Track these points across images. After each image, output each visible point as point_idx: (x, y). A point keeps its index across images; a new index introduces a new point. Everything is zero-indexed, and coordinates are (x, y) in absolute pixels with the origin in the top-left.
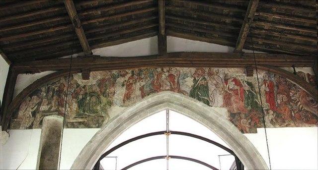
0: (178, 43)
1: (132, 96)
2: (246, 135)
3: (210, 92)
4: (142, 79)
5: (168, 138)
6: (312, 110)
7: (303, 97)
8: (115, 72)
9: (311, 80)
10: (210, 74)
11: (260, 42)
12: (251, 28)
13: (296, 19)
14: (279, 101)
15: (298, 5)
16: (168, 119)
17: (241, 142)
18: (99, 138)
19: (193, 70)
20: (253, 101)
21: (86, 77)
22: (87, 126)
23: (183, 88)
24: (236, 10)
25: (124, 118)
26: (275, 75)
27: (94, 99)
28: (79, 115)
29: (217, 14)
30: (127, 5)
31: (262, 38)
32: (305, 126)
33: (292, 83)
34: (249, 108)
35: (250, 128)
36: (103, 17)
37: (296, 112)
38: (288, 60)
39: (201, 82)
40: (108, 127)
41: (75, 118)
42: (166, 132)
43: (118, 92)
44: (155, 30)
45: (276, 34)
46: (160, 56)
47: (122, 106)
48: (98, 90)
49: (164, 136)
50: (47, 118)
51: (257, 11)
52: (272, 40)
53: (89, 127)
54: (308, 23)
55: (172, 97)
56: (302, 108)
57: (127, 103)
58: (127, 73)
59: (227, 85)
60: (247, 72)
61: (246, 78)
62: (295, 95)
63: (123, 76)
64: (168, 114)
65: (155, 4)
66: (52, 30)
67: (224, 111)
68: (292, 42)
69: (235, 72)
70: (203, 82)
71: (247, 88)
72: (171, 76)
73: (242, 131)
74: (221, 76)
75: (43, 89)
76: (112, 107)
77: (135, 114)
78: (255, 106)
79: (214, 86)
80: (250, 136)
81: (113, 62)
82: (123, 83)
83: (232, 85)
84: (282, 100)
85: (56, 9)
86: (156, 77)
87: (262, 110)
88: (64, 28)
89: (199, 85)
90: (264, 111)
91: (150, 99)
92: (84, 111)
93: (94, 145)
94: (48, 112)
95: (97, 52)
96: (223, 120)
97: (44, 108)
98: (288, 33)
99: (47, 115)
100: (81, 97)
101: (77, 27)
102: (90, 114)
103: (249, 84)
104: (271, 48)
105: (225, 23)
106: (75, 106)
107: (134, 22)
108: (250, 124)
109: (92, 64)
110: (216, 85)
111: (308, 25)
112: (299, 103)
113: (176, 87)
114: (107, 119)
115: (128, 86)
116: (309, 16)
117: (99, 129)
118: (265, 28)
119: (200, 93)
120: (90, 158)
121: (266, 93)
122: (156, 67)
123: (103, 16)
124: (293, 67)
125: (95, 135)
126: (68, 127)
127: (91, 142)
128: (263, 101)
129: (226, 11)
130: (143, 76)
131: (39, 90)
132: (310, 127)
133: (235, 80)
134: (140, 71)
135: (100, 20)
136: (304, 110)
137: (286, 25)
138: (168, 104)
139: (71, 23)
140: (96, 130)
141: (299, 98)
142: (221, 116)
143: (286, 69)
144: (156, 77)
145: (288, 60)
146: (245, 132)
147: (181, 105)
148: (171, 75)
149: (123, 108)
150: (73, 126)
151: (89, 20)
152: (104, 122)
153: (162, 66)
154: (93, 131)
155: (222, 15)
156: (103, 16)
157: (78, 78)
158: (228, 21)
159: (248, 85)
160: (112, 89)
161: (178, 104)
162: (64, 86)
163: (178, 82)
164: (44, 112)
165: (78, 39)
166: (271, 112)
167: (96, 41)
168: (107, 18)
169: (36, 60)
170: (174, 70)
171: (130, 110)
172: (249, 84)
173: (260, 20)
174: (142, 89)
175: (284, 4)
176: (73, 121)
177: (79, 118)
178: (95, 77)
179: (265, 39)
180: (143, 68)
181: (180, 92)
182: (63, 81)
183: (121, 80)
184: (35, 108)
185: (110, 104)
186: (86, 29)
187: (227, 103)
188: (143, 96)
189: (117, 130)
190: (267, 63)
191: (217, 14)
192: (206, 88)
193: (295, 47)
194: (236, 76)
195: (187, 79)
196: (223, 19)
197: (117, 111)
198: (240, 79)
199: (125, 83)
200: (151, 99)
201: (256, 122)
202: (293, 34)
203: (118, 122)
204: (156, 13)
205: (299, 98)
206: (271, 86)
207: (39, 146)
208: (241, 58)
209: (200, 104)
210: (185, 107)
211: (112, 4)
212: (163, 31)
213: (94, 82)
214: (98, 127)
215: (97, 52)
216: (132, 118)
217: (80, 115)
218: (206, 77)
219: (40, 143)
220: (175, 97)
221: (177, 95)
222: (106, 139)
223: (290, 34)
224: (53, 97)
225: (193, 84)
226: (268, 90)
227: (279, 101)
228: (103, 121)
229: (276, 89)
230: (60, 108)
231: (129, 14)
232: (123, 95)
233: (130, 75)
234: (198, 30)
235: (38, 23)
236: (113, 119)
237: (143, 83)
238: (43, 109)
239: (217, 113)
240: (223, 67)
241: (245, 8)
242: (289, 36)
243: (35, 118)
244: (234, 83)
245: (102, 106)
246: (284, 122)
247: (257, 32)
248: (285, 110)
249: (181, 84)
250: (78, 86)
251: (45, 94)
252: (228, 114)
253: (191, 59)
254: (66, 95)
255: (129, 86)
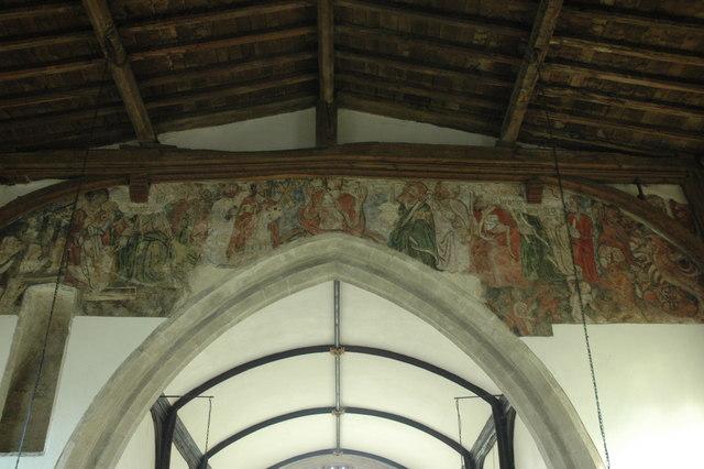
0: (363, 125)
1: (249, 243)
2: (525, 339)
3: (439, 239)
4: (275, 203)
5: (338, 364)
6: (684, 282)
7: (661, 253)
8: (210, 186)
9: (680, 215)
10: (440, 196)
11: (558, 125)
12: (541, 84)
13: (650, 56)
14: (604, 262)
15: (657, 15)
16: (337, 313)
17: (513, 356)
18: (163, 341)
19: (398, 185)
20: (541, 259)
21: (139, 195)
22: (134, 310)
23: (374, 227)
24: (508, 32)
25: (226, 296)
26: (593, 202)
27: (155, 248)
28: (116, 285)
29: (458, 45)
30: (240, 13)
31: (563, 111)
32: (668, 321)
33: (633, 222)
34: (534, 276)
35: (536, 324)
36: (184, 43)
37: (645, 287)
38: (625, 167)
39: (417, 213)
40: (184, 320)
41: (107, 290)
42: (333, 346)
43: (215, 234)
44: (309, 93)
45: (598, 99)
46: (320, 149)
47: (224, 266)
48: (168, 226)
49: (327, 357)
50: (35, 290)
51: (558, 33)
52: (587, 116)
53: (140, 314)
54: (678, 64)
55: (347, 248)
56: (659, 278)
57: (235, 258)
58: (239, 189)
59: (479, 221)
60: (528, 193)
61: (525, 207)
62: (643, 249)
63: (231, 195)
64: (337, 298)
65: (310, 18)
66: (53, 70)
67: (473, 283)
68: (635, 120)
69: (500, 193)
70: (424, 215)
71: (527, 229)
72: (346, 199)
73: (517, 332)
74: (466, 202)
75: (33, 221)
76: (199, 268)
77: (256, 287)
78: (548, 271)
79: (449, 225)
80: (534, 344)
81: (206, 162)
82: (229, 211)
83: (491, 222)
84: (612, 258)
85: (61, 10)
86: (308, 200)
87: (565, 282)
88: (83, 66)
89: (413, 220)
90: (570, 284)
91: (292, 252)
92: (130, 276)
93: (150, 358)
94: (39, 277)
95: (171, 138)
96: (470, 304)
97: (29, 265)
98: (627, 97)
99: (37, 283)
100: (123, 242)
101: (115, 62)
102: (142, 281)
103: (533, 221)
104: (584, 138)
105: (476, 71)
106: (107, 263)
107: (258, 65)
108: (535, 314)
109: (158, 163)
110: (453, 222)
111: (676, 72)
112: (653, 267)
113: (356, 224)
114: (186, 295)
115: (242, 218)
116: (683, 46)
117: (164, 319)
118: (572, 84)
119: (413, 238)
120: (137, 391)
121: (572, 242)
122: (310, 177)
123: (183, 39)
124: (637, 182)
125: (153, 336)
126: (85, 312)
127: (141, 349)
128: (563, 260)
129: (480, 34)
130: (277, 197)
131: (22, 223)
132: (680, 323)
133: (499, 211)
134: (273, 184)
135: (174, 51)
136: (665, 282)
137: (625, 72)
138: (337, 266)
139: (100, 56)
140: (153, 323)
141: (651, 255)
142: (464, 293)
143: (620, 187)
144: (308, 200)
145: (625, 167)
146: (522, 332)
147: (368, 268)
148: (346, 195)
149: (224, 271)
150: (99, 309)
151: (148, 49)
152: (178, 304)
153: (325, 173)
154: (149, 324)
155: (470, 47)
156: (183, 39)
157: (120, 198)
158: (484, 63)
159: (530, 223)
160: (202, 226)
161: (361, 266)
162: (86, 216)
163: (362, 212)
164: (30, 274)
165: (121, 103)
166: (586, 287)
167: (165, 117)
168: (192, 48)
169: (18, 150)
170: (353, 185)
171: (241, 276)
172: (533, 221)
173: (560, 61)
174: (273, 227)
175: (625, 12)
176: (102, 298)
177: (117, 291)
178: (163, 195)
179: (571, 113)
180: (278, 178)
181: (366, 234)
182: (82, 203)
183: (224, 205)
184: (8, 265)
185: (195, 259)
186: (140, 75)
187: (479, 264)
188: (276, 242)
189: (212, 323)
190: (575, 173)
191: (458, 45)
192: (429, 229)
193: (640, 134)
194: (503, 202)
195: (383, 206)
196: (472, 62)
197: (212, 279)
198: (510, 208)
199: (234, 213)
200: (295, 252)
201: (549, 310)
202: (639, 99)
203: (212, 302)
204: (313, 46)
205: (651, 255)
206: (585, 226)
207: (7, 357)
208: (513, 158)
209: (413, 265)
210: (377, 272)
211: (205, 10)
212: (328, 92)
213: (159, 208)
214: (162, 314)
215: (171, 138)
216: (248, 297)
217: (120, 284)
218: (429, 203)
219: (12, 350)
220: (353, 248)
221: (359, 244)
222: (182, 348)
223: (632, 98)
224: (54, 239)
225: (397, 217)
226: (576, 235)
227: (604, 262)
228: (174, 300)
229: (595, 232)
230: (71, 268)
231: (247, 40)
232: (228, 240)
233: (245, 194)
234: (413, 91)
235: (13, 47)
236: (201, 296)
237: (276, 214)
238: (27, 269)
239: (455, 287)
240: (469, 179)
241: (526, 26)
242: (631, 104)
243: (5, 288)
244: (495, 217)
245: (174, 264)
246: (617, 309)
247: (552, 93)
248: (619, 282)
249: (368, 216)
250: (119, 216)
251: (36, 234)
252: (481, 290)
253: (395, 159)
254: (86, 236)
255: (242, 219)
